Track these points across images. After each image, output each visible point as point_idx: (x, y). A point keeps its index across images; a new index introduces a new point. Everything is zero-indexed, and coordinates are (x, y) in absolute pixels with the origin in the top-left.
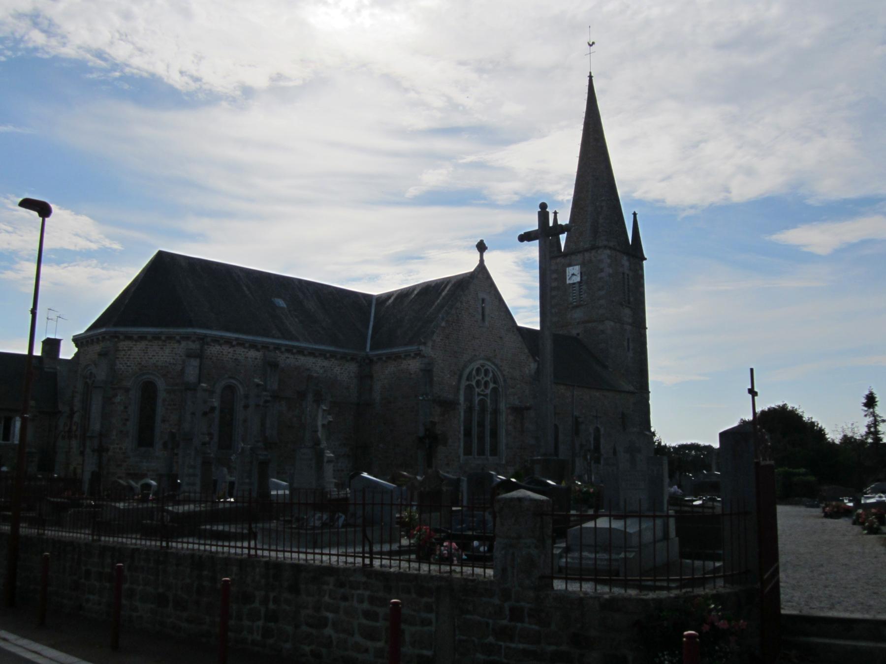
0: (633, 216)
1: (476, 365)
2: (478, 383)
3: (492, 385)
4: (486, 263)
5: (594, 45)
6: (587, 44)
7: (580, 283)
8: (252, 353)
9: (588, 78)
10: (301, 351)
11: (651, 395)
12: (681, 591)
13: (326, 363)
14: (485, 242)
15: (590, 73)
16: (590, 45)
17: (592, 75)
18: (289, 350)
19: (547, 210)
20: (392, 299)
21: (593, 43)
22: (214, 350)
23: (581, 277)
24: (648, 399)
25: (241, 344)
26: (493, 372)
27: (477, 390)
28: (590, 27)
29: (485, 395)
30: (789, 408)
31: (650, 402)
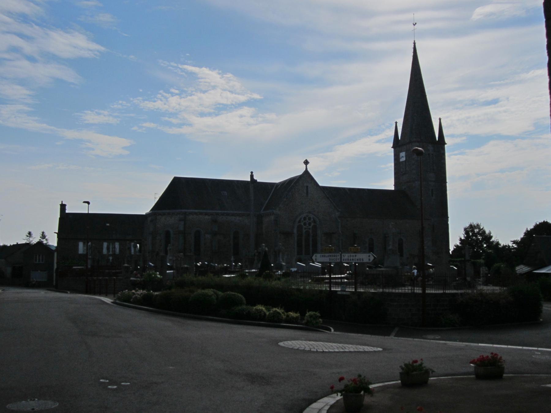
0: (439, 120)
1: (304, 215)
2: (305, 224)
3: (312, 224)
4: (308, 170)
5: (416, 25)
6: (413, 25)
7: (405, 161)
8: (207, 217)
9: (413, 44)
10: (228, 215)
11: (449, 219)
12: (273, 311)
13: (241, 218)
14: (308, 160)
15: (414, 41)
16: (414, 25)
17: (415, 42)
18: (223, 214)
19: (253, 174)
20: (280, 186)
21: (416, 23)
22: (191, 217)
23: (406, 158)
24: (447, 221)
25: (201, 214)
26: (313, 218)
27: (304, 227)
28: (414, 14)
29: (309, 229)
30: (538, 223)
31: (449, 223)
